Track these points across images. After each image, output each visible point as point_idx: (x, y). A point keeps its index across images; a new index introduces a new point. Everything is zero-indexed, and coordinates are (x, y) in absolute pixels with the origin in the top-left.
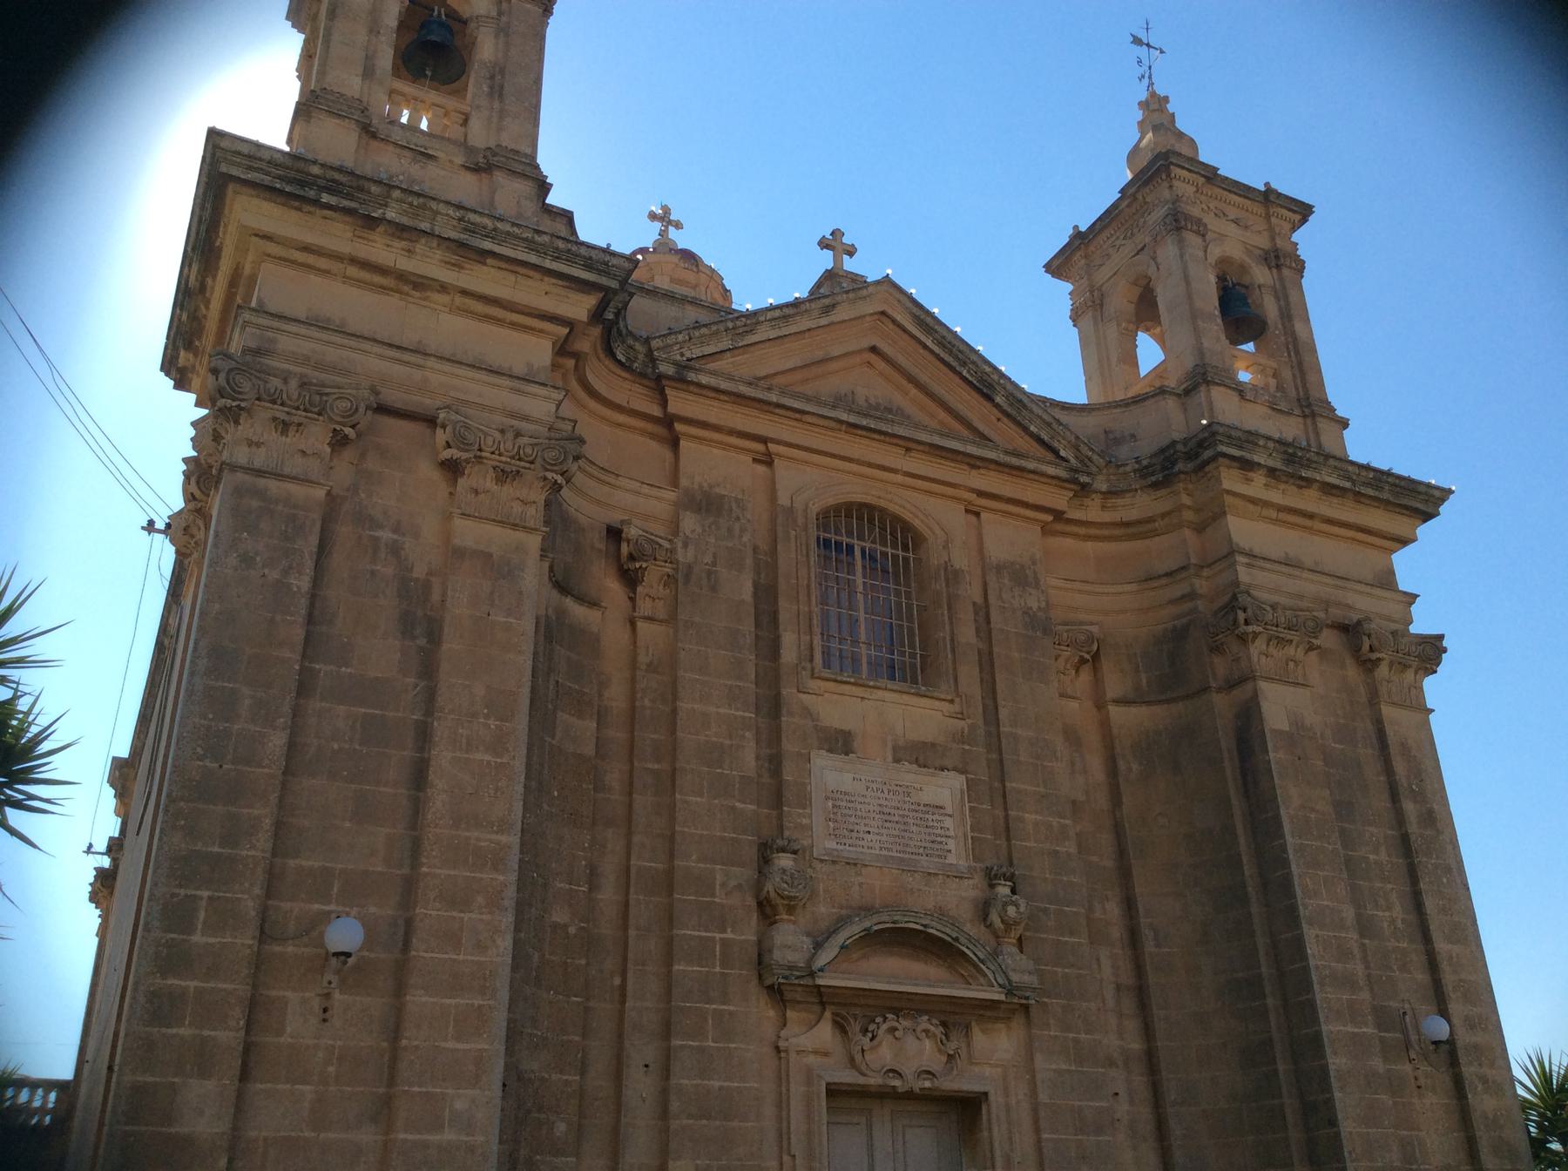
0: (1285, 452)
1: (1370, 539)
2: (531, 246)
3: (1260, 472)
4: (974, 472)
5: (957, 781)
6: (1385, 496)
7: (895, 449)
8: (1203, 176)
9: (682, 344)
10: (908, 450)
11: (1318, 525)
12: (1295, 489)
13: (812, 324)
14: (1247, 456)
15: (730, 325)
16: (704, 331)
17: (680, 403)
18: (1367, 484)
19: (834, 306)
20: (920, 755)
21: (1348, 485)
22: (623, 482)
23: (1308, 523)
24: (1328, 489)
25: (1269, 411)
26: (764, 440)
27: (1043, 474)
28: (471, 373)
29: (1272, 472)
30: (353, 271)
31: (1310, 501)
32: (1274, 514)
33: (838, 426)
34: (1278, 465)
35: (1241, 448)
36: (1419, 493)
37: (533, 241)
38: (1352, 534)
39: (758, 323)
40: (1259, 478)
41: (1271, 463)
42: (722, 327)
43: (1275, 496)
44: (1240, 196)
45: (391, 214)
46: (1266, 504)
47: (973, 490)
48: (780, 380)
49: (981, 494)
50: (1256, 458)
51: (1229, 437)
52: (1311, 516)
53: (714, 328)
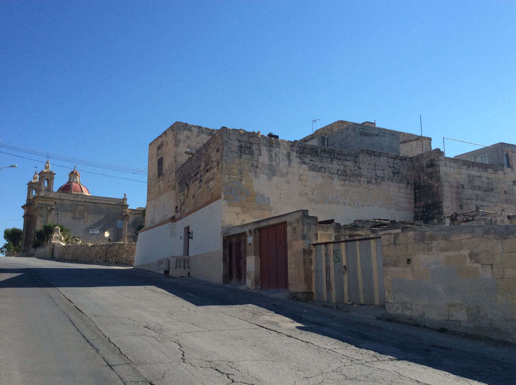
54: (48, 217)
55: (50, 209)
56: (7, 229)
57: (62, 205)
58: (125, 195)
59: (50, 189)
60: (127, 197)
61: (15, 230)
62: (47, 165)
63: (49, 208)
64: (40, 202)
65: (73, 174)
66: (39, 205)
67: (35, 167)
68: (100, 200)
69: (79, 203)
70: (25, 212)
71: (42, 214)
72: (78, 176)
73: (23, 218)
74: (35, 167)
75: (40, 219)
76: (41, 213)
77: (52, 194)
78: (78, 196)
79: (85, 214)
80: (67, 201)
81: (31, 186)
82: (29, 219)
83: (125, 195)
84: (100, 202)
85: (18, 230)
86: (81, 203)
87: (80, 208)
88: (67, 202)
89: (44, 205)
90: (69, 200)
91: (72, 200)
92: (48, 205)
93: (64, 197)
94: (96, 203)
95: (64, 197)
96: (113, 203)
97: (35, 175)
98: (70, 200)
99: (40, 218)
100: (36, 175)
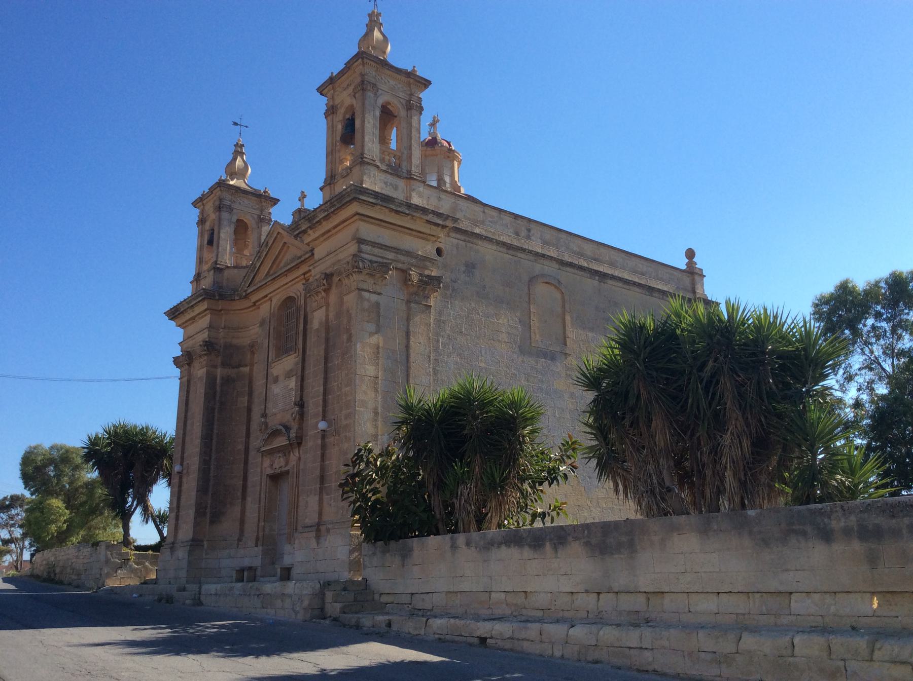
0: (307, 220)
1: (348, 222)
2: (194, 299)
3: (309, 230)
4: (300, 269)
5: (294, 379)
6: (338, 205)
7: (284, 278)
8: (329, 85)
9: (244, 285)
10: (286, 275)
11: (334, 231)
12: (320, 226)
13: (265, 253)
14: (300, 230)
15: (250, 271)
16: (246, 277)
17: (254, 298)
18: (330, 208)
19: (267, 243)
20: (288, 375)
21: (326, 213)
22: (250, 328)
23: (331, 233)
24: (326, 218)
25: (344, 179)
26: (266, 296)
27: (307, 259)
28: (199, 334)
29: (310, 228)
30: (189, 323)
31: (327, 226)
32: (322, 239)
33: (273, 281)
34: (309, 225)
35: (298, 229)
36: (344, 195)
37: (193, 299)
38: (342, 226)
39: (255, 264)
40: (310, 232)
41: (306, 226)
42: (249, 273)
43: (317, 234)
44: (343, 75)
45: (182, 310)
46: (317, 238)
47: (302, 274)
48: (271, 272)
49: (304, 274)
50: (303, 228)
51: (293, 229)
52: (329, 231)
53: (247, 275)
54: (408, 334)
55: (420, 281)
56: (35, 448)
57: (470, 267)
58: (690, 254)
59: (404, 165)
60: (700, 262)
61: (126, 432)
62: (239, 162)
63: (414, 275)
64: (368, 231)
65: (436, 147)
66: (364, 247)
67: (235, 124)
68: (612, 264)
69: (539, 267)
70: (187, 338)
71: (378, 305)
72: (456, 164)
73: (177, 372)
74: (235, 124)
75: (374, 340)
76: (374, 298)
77: (420, 195)
78: (529, 230)
79: (571, 332)
80: (487, 245)
81: (228, 203)
82: (219, 372)
83: (690, 254)
84: (617, 273)
85: (144, 432)
86: (550, 268)
87: (540, 289)
88: (488, 252)
89: (391, 255)
90: (499, 243)
91: (509, 247)
92: (408, 253)
93: (475, 223)
94: (603, 276)
95: (475, 223)
96: (659, 287)
97: (235, 159)
98: (504, 244)
99: (371, 334)
100: (239, 158)
